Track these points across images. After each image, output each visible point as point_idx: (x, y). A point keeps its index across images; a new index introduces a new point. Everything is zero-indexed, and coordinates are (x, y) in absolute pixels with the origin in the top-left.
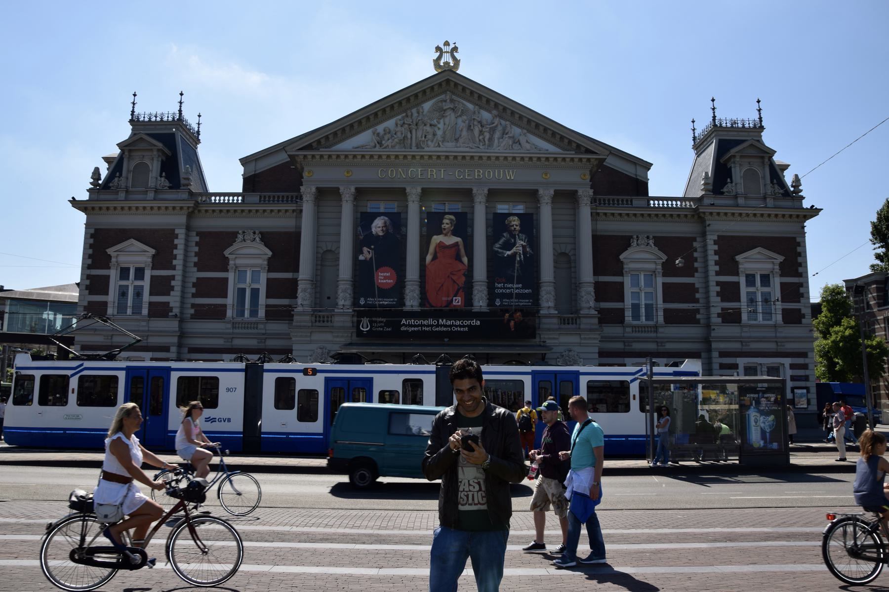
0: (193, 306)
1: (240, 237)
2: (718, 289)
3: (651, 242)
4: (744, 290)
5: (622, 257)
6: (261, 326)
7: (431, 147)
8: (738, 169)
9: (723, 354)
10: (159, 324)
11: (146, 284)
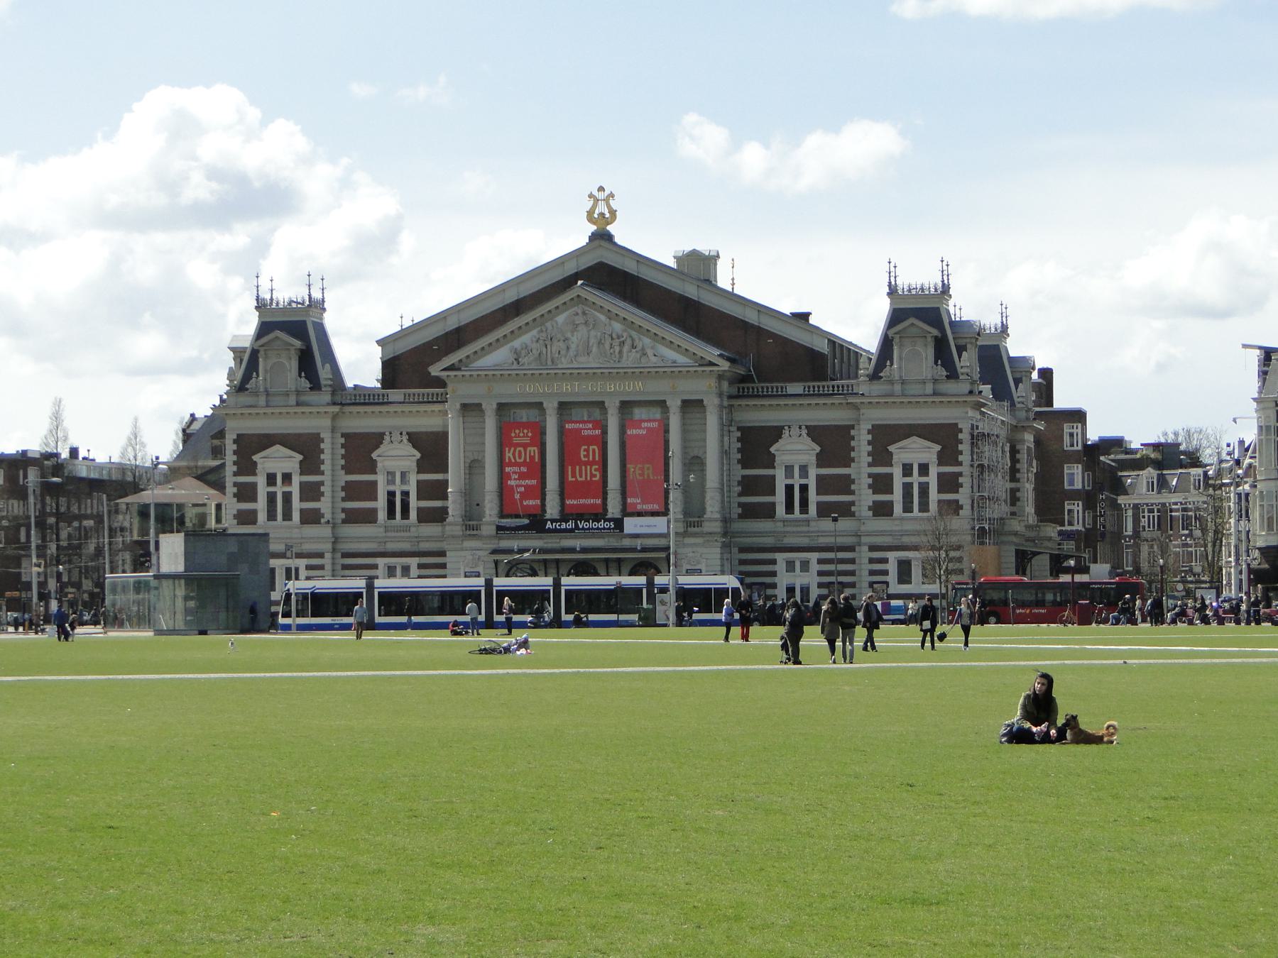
0: (343, 510)
1: (387, 438)
2: (870, 481)
3: (804, 432)
5: (772, 450)
6: (413, 529)
7: (564, 363)
9: (873, 548)
10: (311, 530)
11: (295, 489)
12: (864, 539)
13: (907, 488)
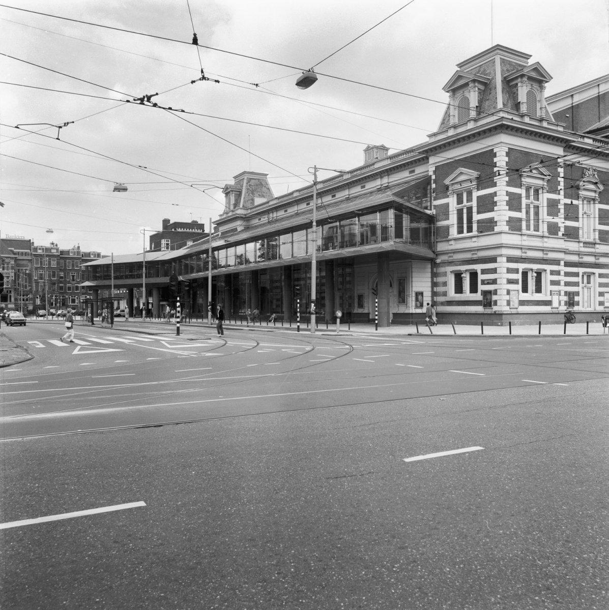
2: (507, 198)
4: (524, 201)
8: (525, 87)
9: (510, 259)
12: (504, 251)
13: (528, 206)
